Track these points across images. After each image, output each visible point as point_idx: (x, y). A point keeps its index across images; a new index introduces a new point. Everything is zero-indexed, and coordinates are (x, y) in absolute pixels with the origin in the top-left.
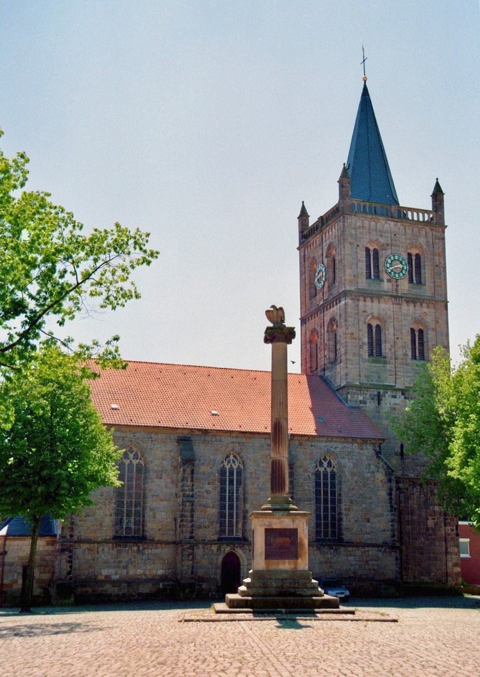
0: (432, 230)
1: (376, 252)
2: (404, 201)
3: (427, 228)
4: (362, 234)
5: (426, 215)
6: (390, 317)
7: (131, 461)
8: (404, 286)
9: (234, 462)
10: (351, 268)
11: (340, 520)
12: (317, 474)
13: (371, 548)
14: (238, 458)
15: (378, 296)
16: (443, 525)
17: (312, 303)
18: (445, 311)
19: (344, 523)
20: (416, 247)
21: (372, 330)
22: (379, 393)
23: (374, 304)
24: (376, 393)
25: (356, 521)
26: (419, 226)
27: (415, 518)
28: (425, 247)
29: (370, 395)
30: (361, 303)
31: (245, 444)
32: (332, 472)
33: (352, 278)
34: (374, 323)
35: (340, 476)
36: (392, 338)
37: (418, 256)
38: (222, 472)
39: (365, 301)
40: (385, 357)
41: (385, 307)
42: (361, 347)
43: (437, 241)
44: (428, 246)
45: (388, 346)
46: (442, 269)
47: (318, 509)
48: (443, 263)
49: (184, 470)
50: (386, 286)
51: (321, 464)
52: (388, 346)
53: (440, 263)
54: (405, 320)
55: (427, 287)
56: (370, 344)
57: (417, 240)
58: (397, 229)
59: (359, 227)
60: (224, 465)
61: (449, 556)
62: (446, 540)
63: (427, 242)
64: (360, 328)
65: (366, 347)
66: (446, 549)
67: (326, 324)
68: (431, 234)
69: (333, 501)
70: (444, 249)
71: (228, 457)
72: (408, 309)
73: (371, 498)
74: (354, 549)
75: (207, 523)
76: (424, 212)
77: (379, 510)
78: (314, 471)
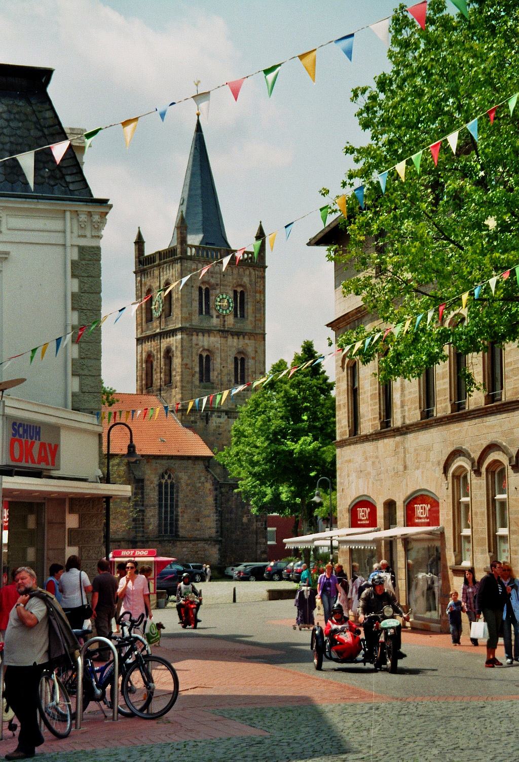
0: (254, 270)
1: (207, 290)
3: (250, 268)
6: (217, 349)
8: (230, 320)
10: (187, 307)
11: (177, 520)
15: (208, 332)
16: (255, 521)
19: (180, 523)
20: (241, 286)
21: (203, 360)
23: (205, 338)
26: (244, 267)
27: (233, 516)
28: (248, 285)
30: (194, 337)
34: (204, 354)
35: (178, 487)
36: (219, 367)
39: (197, 335)
40: (213, 383)
42: (193, 375)
43: (259, 280)
45: (216, 373)
46: (262, 305)
47: (160, 513)
48: (263, 299)
50: (215, 321)
51: (163, 477)
52: (216, 373)
53: (261, 300)
54: (230, 351)
55: (248, 322)
57: (242, 279)
61: (259, 546)
62: (257, 534)
63: (251, 281)
65: (197, 376)
66: (257, 540)
67: (162, 350)
69: (172, 506)
70: (264, 286)
77: (206, 512)
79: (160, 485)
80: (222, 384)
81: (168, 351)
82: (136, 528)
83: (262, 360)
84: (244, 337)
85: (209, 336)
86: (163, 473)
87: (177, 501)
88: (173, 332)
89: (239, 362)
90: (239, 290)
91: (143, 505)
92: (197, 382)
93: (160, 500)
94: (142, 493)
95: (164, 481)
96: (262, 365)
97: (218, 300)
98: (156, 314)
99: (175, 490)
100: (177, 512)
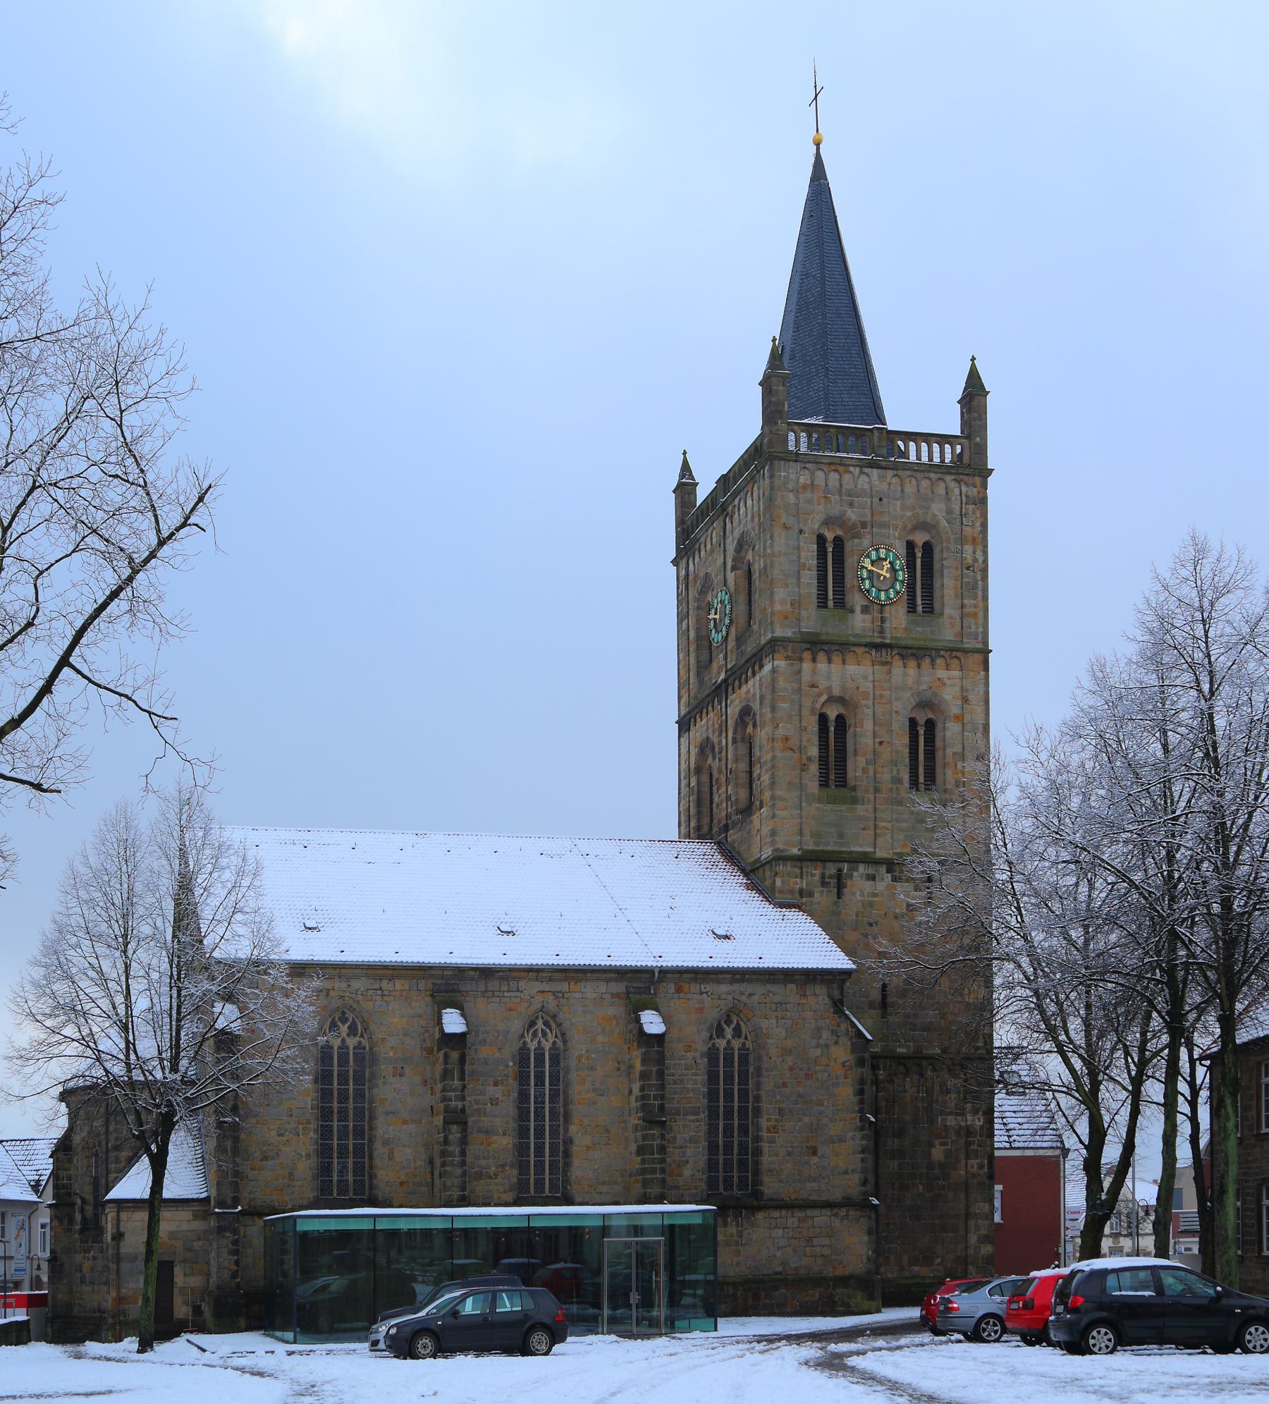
0: (958, 482)
1: (839, 542)
4: (810, 502)
8: (898, 619)
9: (544, 1034)
11: (758, 1152)
13: (817, 1212)
18: (982, 673)
19: (766, 1159)
22: (840, 870)
23: (833, 666)
25: (789, 1154)
26: (932, 475)
28: (944, 523)
31: (566, 995)
32: (743, 1046)
36: (870, 742)
40: (854, 789)
42: (804, 768)
43: (971, 507)
44: (949, 522)
48: (981, 559)
50: (860, 623)
52: (861, 761)
53: (975, 560)
54: (896, 699)
57: (928, 508)
58: (885, 486)
59: (805, 487)
60: (525, 1043)
64: (804, 724)
65: (814, 768)
68: (957, 491)
72: (905, 675)
73: (820, 1103)
74: (784, 1213)
75: (494, 1168)
78: (705, 1049)
79: (712, 1055)
82: (643, 1171)
84: (933, 661)
86: (719, 1024)
87: (758, 1099)
89: (921, 732)
90: (920, 538)
92: (813, 786)
93: (712, 1095)
95: (721, 1043)
96: (979, 735)
100: (758, 1129)
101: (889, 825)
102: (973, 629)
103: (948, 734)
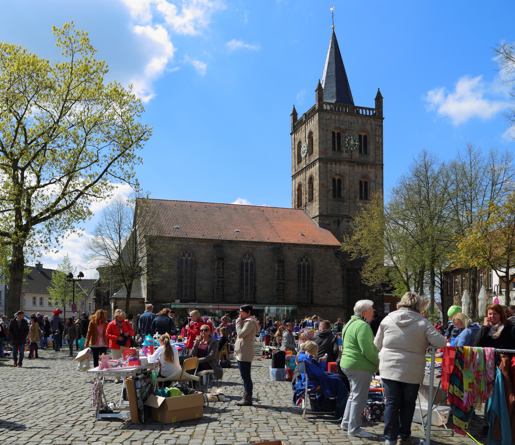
0: (375, 120)
1: (339, 134)
2: (357, 103)
3: (371, 119)
5: (371, 111)
7: (187, 258)
8: (356, 155)
9: (248, 258)
12: (299, 266)
14: (251, 256)
15: (339, 162)
17: (299, 167)
18: (381, 170)
20: (365, 131)
21: (335, 182)
22: (339, 219)
23: (337, 166)
24: (337, 219)
29: (333, 220)
30: (329, 166)
33: (324, 150)
34: (337, 178)
36: (348, 186)
37: (365, 137)
38: (242, 264)
39: (331, 164)
40: (343, 198)
41: (344, 168)
42: (328, 192)
43: (378, 127)
44: (372, 131)
45: (345, 191)
49: (218, 263)
50: (345, 155)
51: (302, 260)
52: (345, 191)
53: (379, 141)
56: (334, 190)
58: (352, 120)
59: (328, 119)
60: (243, 261)
63: (372, 128)
64: (328, 180)
65: (331, 192)
71: (245, 256)
72: (358, 170)
76: (370, 109)
80: (350, 199)
81: (311, 179)
83: (381, 183)
85: (340, 165)
88: (313, 163)
90: (363, 134)
91: (283, 279)
92: (331, 197)
94: (283, 271)
96: (380, 186)
97: (347, 140)
98: (303, 156)
99: (311, 270)
101: (353, 208)
102: (379, 159)
103: (371, 185)
